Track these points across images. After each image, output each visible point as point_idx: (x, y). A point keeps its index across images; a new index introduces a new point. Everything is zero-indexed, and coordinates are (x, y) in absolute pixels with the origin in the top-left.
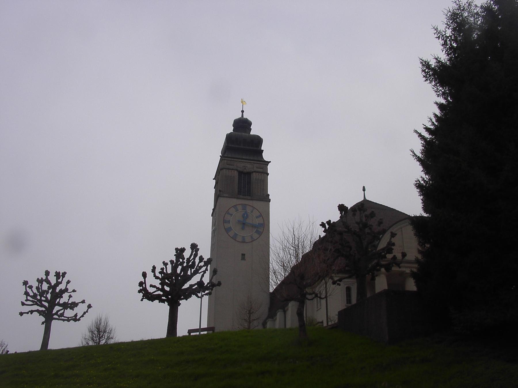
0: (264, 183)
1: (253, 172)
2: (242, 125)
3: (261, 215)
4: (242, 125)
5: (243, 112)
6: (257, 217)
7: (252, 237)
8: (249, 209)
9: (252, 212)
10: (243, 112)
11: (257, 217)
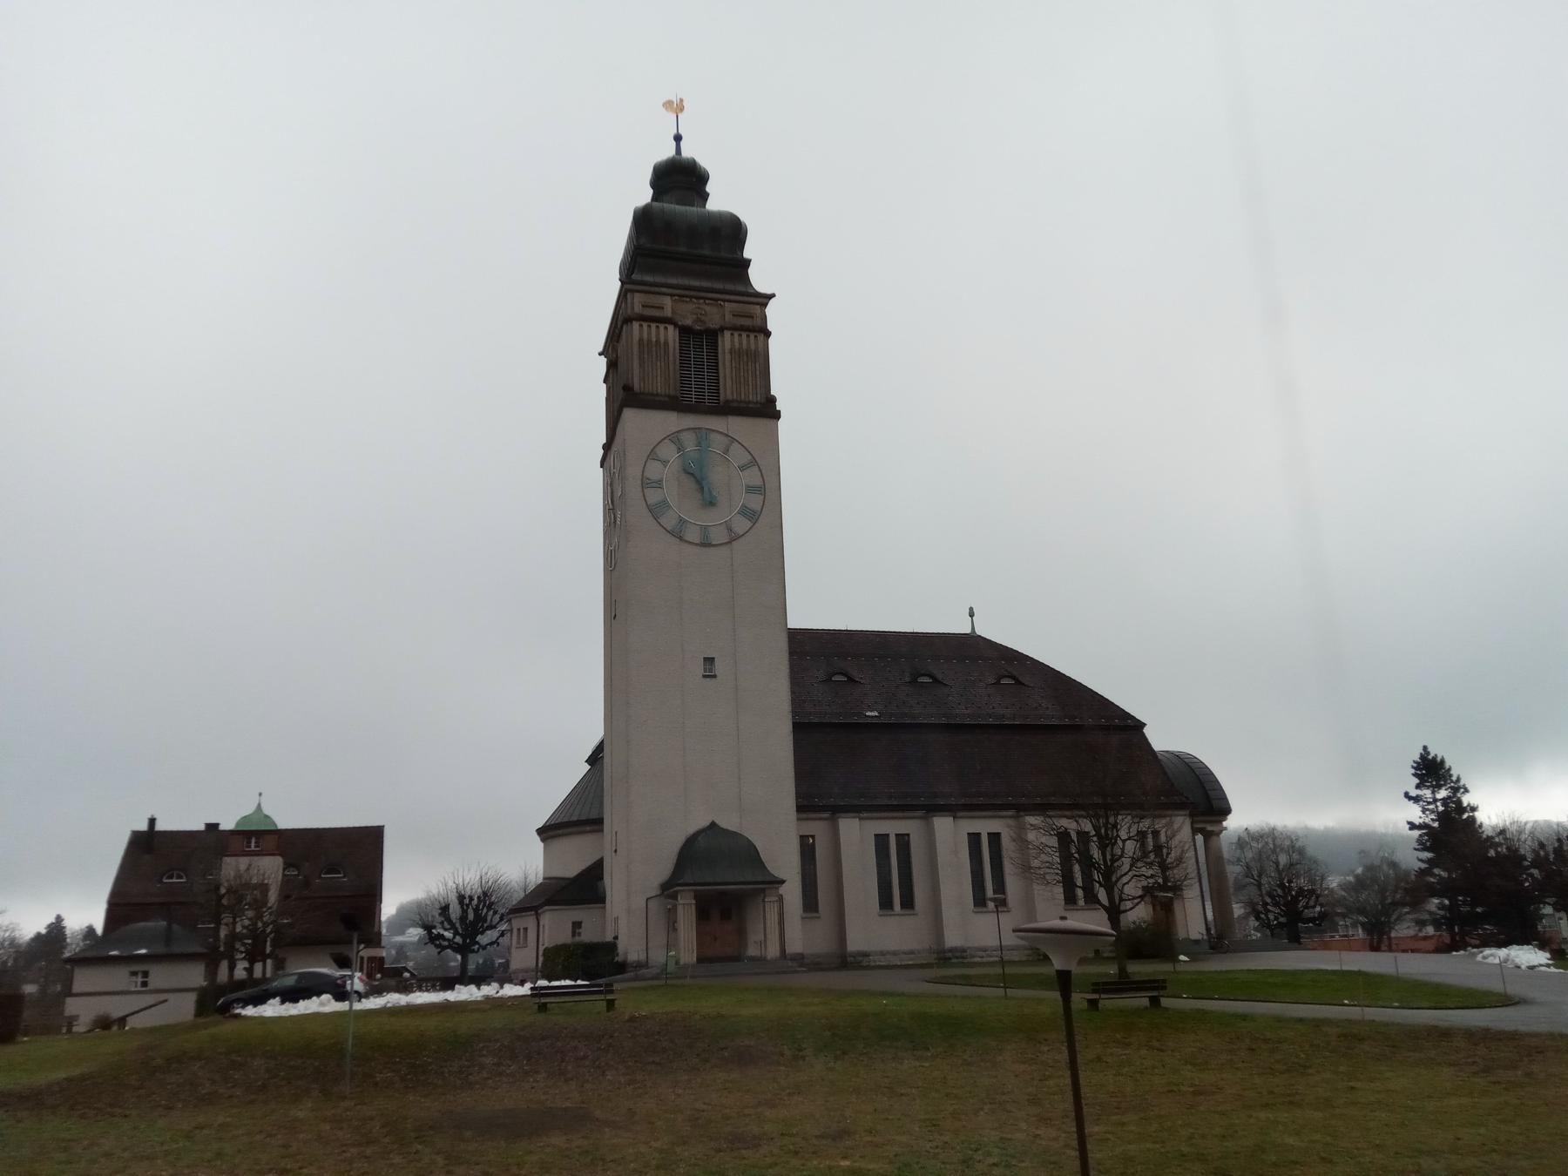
0: (759, 364)
1: (722, 329)
2: (679, 178)
3: (754, 462)
4: (679, 178)
5: (678, 138)
6: (742, 468)
7: (730, 530)
8: (717, 443)
9: (726, 451)
10: (678, 138)
11: (742, 468)
